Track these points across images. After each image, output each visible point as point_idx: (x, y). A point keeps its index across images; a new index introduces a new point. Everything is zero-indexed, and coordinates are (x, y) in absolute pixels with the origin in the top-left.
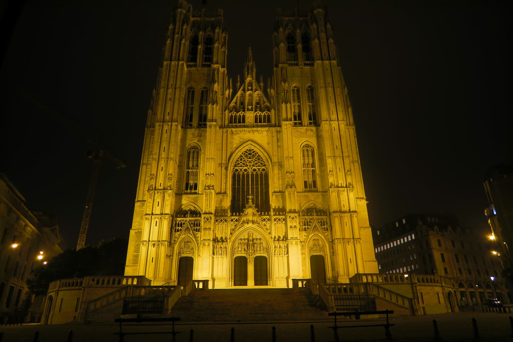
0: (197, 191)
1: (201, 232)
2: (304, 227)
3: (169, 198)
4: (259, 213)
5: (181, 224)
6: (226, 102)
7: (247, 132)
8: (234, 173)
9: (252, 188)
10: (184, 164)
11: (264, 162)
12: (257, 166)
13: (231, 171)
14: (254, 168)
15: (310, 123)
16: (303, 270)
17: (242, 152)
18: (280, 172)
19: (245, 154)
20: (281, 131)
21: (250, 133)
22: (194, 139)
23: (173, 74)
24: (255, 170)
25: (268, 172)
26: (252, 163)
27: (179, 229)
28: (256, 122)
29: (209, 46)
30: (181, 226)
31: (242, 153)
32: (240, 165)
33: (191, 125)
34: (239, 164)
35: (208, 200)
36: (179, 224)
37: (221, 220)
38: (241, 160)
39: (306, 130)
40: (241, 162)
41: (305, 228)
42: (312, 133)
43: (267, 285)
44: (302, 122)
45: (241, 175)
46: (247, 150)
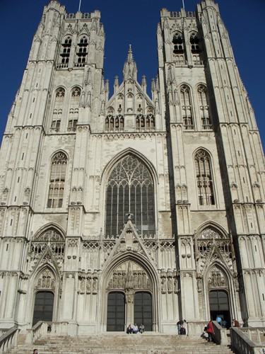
0: (61, 209)
4: (142, 235)
15: (205, 127)
16: (200, 310)
24: (136, 182)
29: (83, 47)
30: (39, 252)
33: (57, 130)
36: (36, 249)
39: (200, 135)
40: (118, 174)
42: (207, 139)
43: (152, 330)
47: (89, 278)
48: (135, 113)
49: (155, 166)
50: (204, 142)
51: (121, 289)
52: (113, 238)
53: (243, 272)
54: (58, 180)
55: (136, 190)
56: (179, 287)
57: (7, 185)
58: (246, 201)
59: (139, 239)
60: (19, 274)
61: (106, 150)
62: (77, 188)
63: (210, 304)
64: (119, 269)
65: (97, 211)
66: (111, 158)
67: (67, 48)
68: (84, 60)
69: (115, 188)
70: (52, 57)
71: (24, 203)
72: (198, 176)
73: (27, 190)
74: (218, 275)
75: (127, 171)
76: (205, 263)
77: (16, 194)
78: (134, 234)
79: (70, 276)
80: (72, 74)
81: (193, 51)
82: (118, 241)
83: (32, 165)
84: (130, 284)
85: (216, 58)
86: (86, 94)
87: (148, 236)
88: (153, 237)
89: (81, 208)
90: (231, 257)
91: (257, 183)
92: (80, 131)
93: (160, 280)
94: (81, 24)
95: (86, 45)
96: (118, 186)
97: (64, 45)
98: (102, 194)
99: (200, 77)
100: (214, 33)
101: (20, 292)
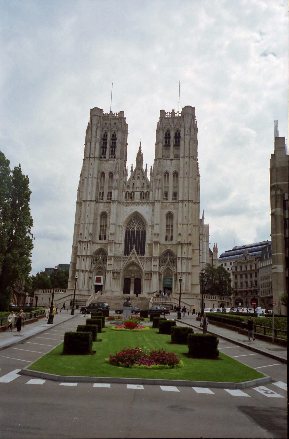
0: (105, 241)
5: (97, 260)
9: (136, 240)
11: (144, 224)
14: (138, 227)
15: (173, 199)
16: (159, 287)
21: (136, 205)
23: (91, 166)
24: (138, 228)
28: (141, 198)
29: (114, 141)
33: (102, 199)
34: (130, 224)
36: (95, 260)
38: (131, 222)
39: (170, 204)
46: (135, 216)
47: (117, 273)
52: (127, 256)
53: (177, 273)
54: (103, 226)
56: (151, 278)
57: (81, 231)
58: (184, 242)
59: (137, 257)
60: (89, 271)
61: (125, 212)
62: (112, 233)
64: (129, 269)
65: (121, 243)
66: (127, 216)
67: (105, 141)
68: (115, 150)
70: (97, 154)
71: (90, 240)
72: (167, 226)
73: (90, 234)
74: (169, 273)
76: (163, 268)
77: (85, 235)
78: (135, 255)
80: (108, 163)
81: (175, 146)
82: (129, 257)
83: (92, 221)
84: (133, 275)
85: (184, 157)
86: (116, 181)
88: (143, 256)
89: (114, 243)
90: (175, 266)
91: (191, 233)
92: (113, 203)
93: (144, 274)
97: (104, 139)
98: (123, 234)
101: (90, 278)
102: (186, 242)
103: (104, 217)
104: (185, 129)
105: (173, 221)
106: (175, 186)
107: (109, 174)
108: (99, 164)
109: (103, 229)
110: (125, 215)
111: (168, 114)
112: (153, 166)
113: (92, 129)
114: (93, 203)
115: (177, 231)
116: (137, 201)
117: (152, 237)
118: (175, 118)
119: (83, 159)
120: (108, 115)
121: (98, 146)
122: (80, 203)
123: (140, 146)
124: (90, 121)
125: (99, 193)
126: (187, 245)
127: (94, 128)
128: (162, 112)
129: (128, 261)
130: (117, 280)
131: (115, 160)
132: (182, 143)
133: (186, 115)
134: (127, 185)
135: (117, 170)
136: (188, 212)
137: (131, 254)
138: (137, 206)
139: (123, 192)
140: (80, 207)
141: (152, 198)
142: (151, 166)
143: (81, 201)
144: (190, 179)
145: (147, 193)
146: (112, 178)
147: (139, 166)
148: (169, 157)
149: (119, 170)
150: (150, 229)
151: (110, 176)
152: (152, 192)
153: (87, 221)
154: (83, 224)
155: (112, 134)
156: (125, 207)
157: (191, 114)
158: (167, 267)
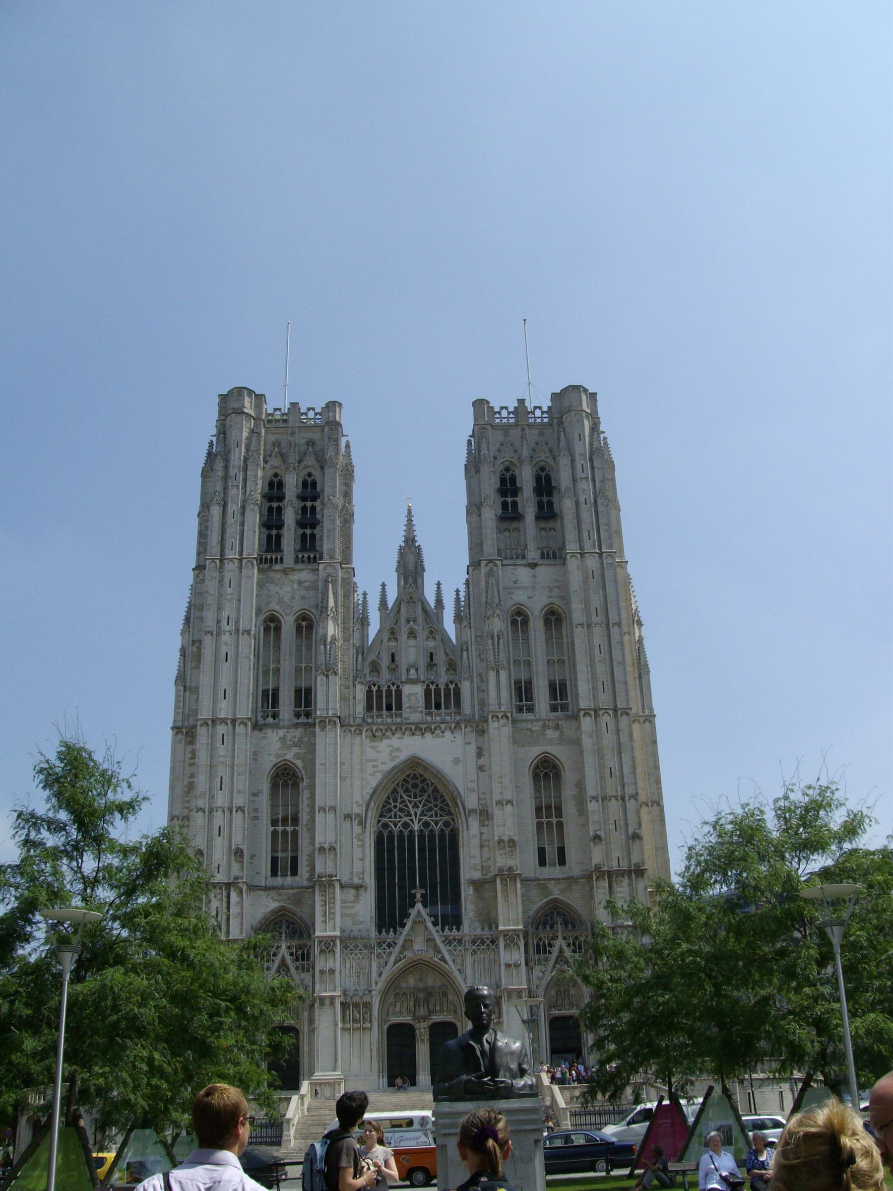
0: (297, 878)
1: (313, 976)
2: (537, 956)
3: (238, 899)
4: (439, 928)
6: (357, 657)
7: (407, 733)
8: (380, 832)
10: (265, 815)
11: (447, 805)
12: (431, 816)
13: (373, 830)
15: (554, 709)
17: (396, 782)
18: (484, 830)
19: (403, 785)
20: (488, 729)
21: (413, 734)
22: (285, 752)
23: (229, 591)
24: (426, 825)
25: (458, 829)
26: (420, 809)
27: (265, 966)
28: (428, 705)
29: (309, 504)
31: (398, 785)
32: (393, 813)
33: (275, 716)
34: (390, 810)
35: (325, 902)
37: (356, 947)
38: (395, 801)
39: (545, 727)
40: (395, 807)
41: (539, 959)
44: (533, 705)
45: (396, 835)
46: (408, 776)
47: (356, 1005)
48: (422, 678)
49: (462, 794)
50: (551, 742)
51: (406, 1019)
54: (285, 821)
55: (427, 839)
58: (615, 866)
59: (436, 935)
61: (371, 761)
62: (327, 846)
63: (552, 1039)
64: (404, 985)
65: (360, 881)
66: (379, 776)
67: (275, 505)
68: (313, 536)
69: (391, 835)
71: (236, 878)
72: (538, 810)
75: (410, 802)
78: (426, 928)
79: (327, 1002)
80: (292, 581)
81: (538, 518)
82: (400, 941)
87: (451, 929)
88: (458, 929)
92: (323, 728)
94: (301, 438)
95: (314, 499)
96: (396, 831)
99: (550, 589)
100: (582, 485)
102: (624, 866)
103: (285, 785)
104: (573, 461)
105: (560, 790)
106: (555, 658)
107: (297, 620)
108: (260, 585)
109: (285, 833)
110: (371, 774)
111: (504, 413)
112: (462, 588)
113: (227, 461)
114: (240, 729)
115: (585, 825)
116: (416, 717)
117: (486, 856)
118: (530, 426)
119: (194, 567)
120: (283, 415)
121: (254, 519)
122: (187, 733)
123: (410, 521)
124: (218, 436)
125: (260, 693)
126: (630, 877)
127: (238, 456)
128: (480, 405)
129: (400, 953)
130: (357, 1033)
131: (321, 567)
132: (566, 505)
133: (573, 413)
134: (371, 658)
135: (331, 603)
136: (620, 753)
137: (407, 928)
138: (417, 738)
139: (354, 685)
140: (189, 748)
141: (473, 706)
142: (457, 591)
143: (191, 722)
144: (612, 630)
145: (452, 687)
146: (309, 638)
147: (411, 590)
148: (524, 557)
149: (336, 602)
150: (474, 824)
151: (299, 629)
152: (472, 682)
153: (221, 799)
154: (204, 812)
155: (301, 480)
156: (368, 743)
157: (589, 411)
158: (558, 966)
